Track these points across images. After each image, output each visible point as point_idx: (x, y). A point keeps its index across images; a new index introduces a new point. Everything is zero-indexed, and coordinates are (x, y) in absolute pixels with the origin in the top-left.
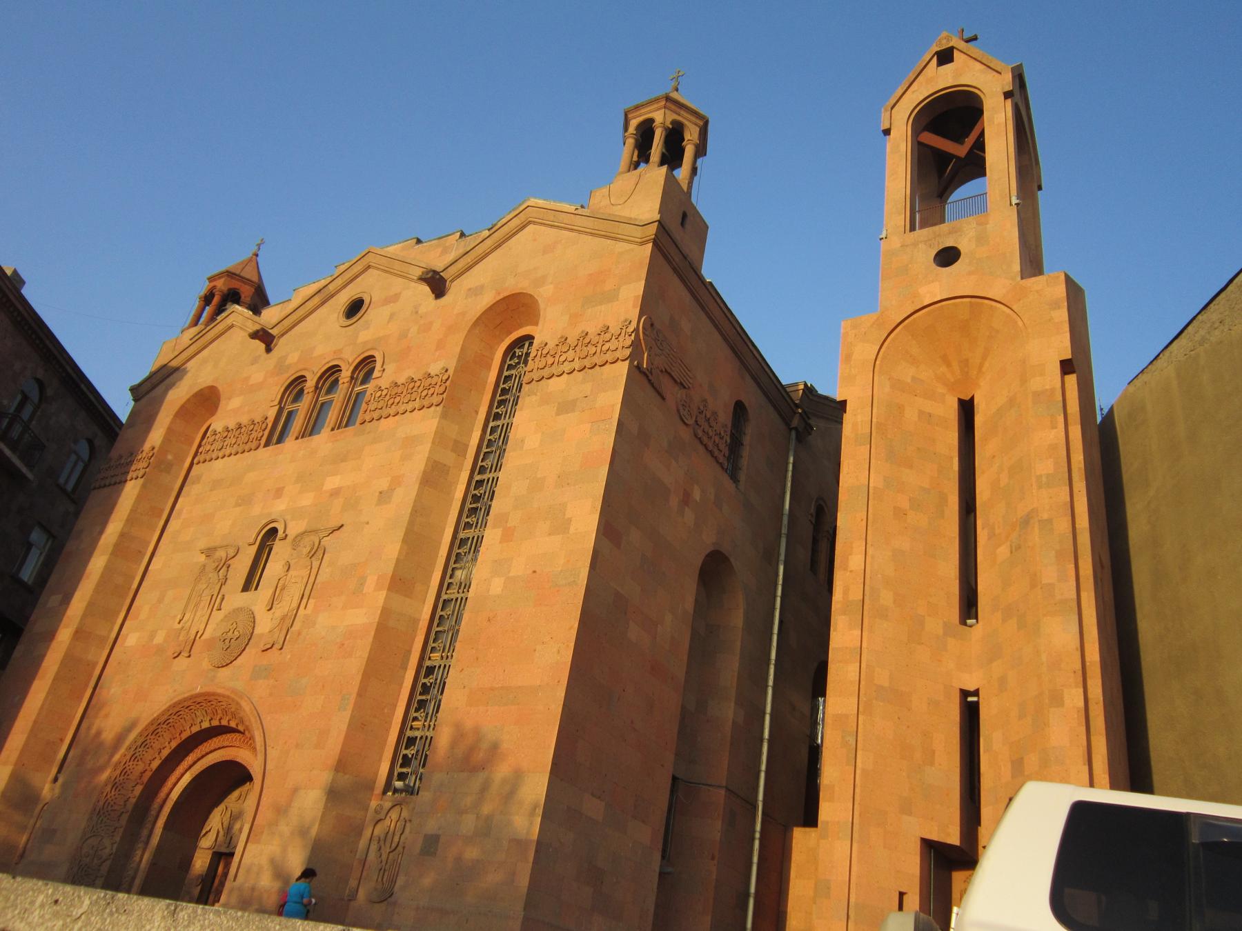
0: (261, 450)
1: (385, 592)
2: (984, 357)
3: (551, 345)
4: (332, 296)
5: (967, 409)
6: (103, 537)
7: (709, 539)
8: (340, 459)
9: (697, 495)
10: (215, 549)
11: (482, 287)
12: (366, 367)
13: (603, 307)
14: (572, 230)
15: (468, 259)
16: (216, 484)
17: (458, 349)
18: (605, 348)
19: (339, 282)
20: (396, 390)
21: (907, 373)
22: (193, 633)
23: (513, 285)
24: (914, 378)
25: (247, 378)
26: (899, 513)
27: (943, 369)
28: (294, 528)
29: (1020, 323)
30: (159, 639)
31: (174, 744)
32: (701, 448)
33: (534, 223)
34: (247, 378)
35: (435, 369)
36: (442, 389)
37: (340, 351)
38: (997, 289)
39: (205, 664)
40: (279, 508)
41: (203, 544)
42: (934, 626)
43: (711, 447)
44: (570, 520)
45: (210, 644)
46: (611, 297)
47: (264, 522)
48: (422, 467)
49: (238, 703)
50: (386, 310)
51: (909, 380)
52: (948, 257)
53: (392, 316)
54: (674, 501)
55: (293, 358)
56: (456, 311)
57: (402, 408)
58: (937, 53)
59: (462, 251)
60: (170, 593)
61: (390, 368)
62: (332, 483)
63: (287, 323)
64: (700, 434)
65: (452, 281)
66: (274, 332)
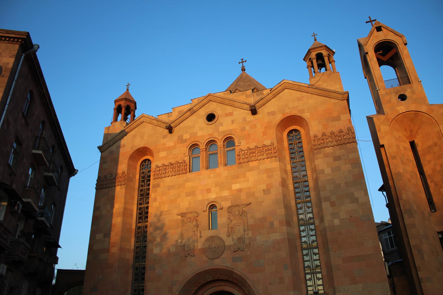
0: (188, 174)
1: (285, 227)
2: (419, 129)
3: (320, 135)
4: (195, 112)
5: (413, 145)
6: (114, 209)
8: (236, 177)
10: (185, 213)
11: (274, 112)
12: (229, 141)
13: (336, 122)
14: (308, 93)
16: (170, 188)
17: (275, 136)
18: (345, 137)
19: (198, 106)
20: (251, 151)
22: (192, 246)
23: (289, 112)
25: (164, 144)
27: (405, 133)
28: (226, 204)
29: (434, 120)
31: (196, 288)
33: (288, 89)
34: (164, 144)
35: (268, 142)
36: (275, 151)
37: (212, 134)
38: (424, 109)
39: (205, 258)
40: (212, 196)
41: (176, 211)
44: (357, 198)
45: (204, 251)
46: (338, 119)
47: (207, 203)
48: (280, 180)
49: (231, 271)
50: (229, 119)
52: (403, 97)
53: (233, 122)
55: (186, 136)
56: (266, 121)
57: (259, 158)
58: (376, 28)
59: (259, 98)
61: (243, 142)
62: (236, 187)
63: (176, 122)
65: (258, 109)
66: (172, 125)
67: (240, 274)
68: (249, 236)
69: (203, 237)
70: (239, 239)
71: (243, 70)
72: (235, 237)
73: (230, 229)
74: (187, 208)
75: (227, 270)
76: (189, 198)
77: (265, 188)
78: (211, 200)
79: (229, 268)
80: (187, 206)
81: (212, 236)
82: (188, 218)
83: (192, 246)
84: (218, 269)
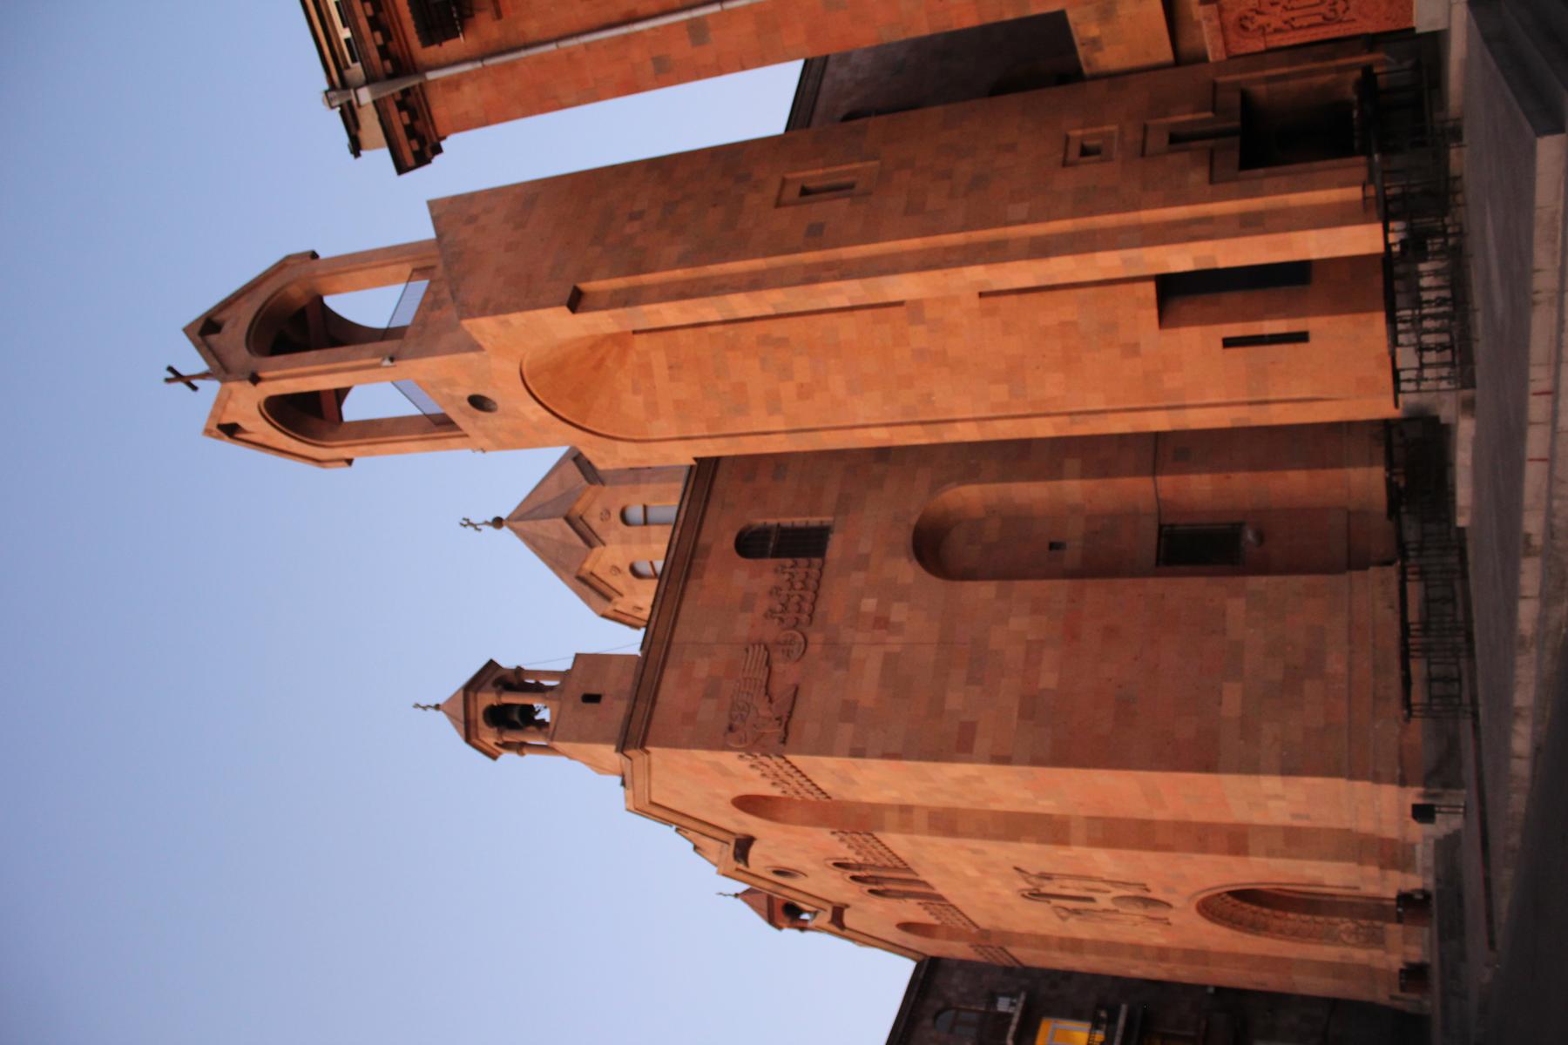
7: (907, 571)
9: (869, 604)
15: (708, 830)
21: (633, 405)
24: (635, 391)
26: (804, 393)
27: (609, 363)
31: (1246, 905)
32: (819, 610)
42: (919, 336)
43: (809, 595)
51: (640, 399)
54: (895, 643)
62: (972, 872)
64: (804, 618)
66: (830, 909)
71: (498, 522)
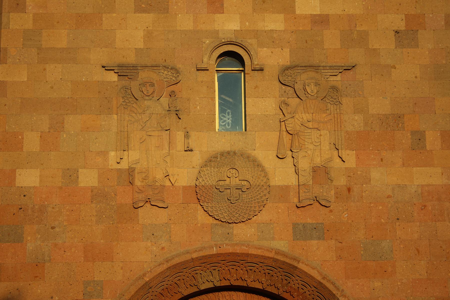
10: (134, 67)
30: (88, 179)
41: (99, 56)
60: (73, 123)
67: (319, 278)
68: (347, 165)
69: (196, 152)
70: (315, 170)
72: (304, 164)
73: (286, 138)
74: (138, 51)
75: (276, 260)
76: (148, 19)
77: (402, 26)
78: (224, 37)
79: (284, 254)
80: (141, 45)
81: (228, 153)
82: (144, 84)
83: (159, 176)
84: (248, 255)
